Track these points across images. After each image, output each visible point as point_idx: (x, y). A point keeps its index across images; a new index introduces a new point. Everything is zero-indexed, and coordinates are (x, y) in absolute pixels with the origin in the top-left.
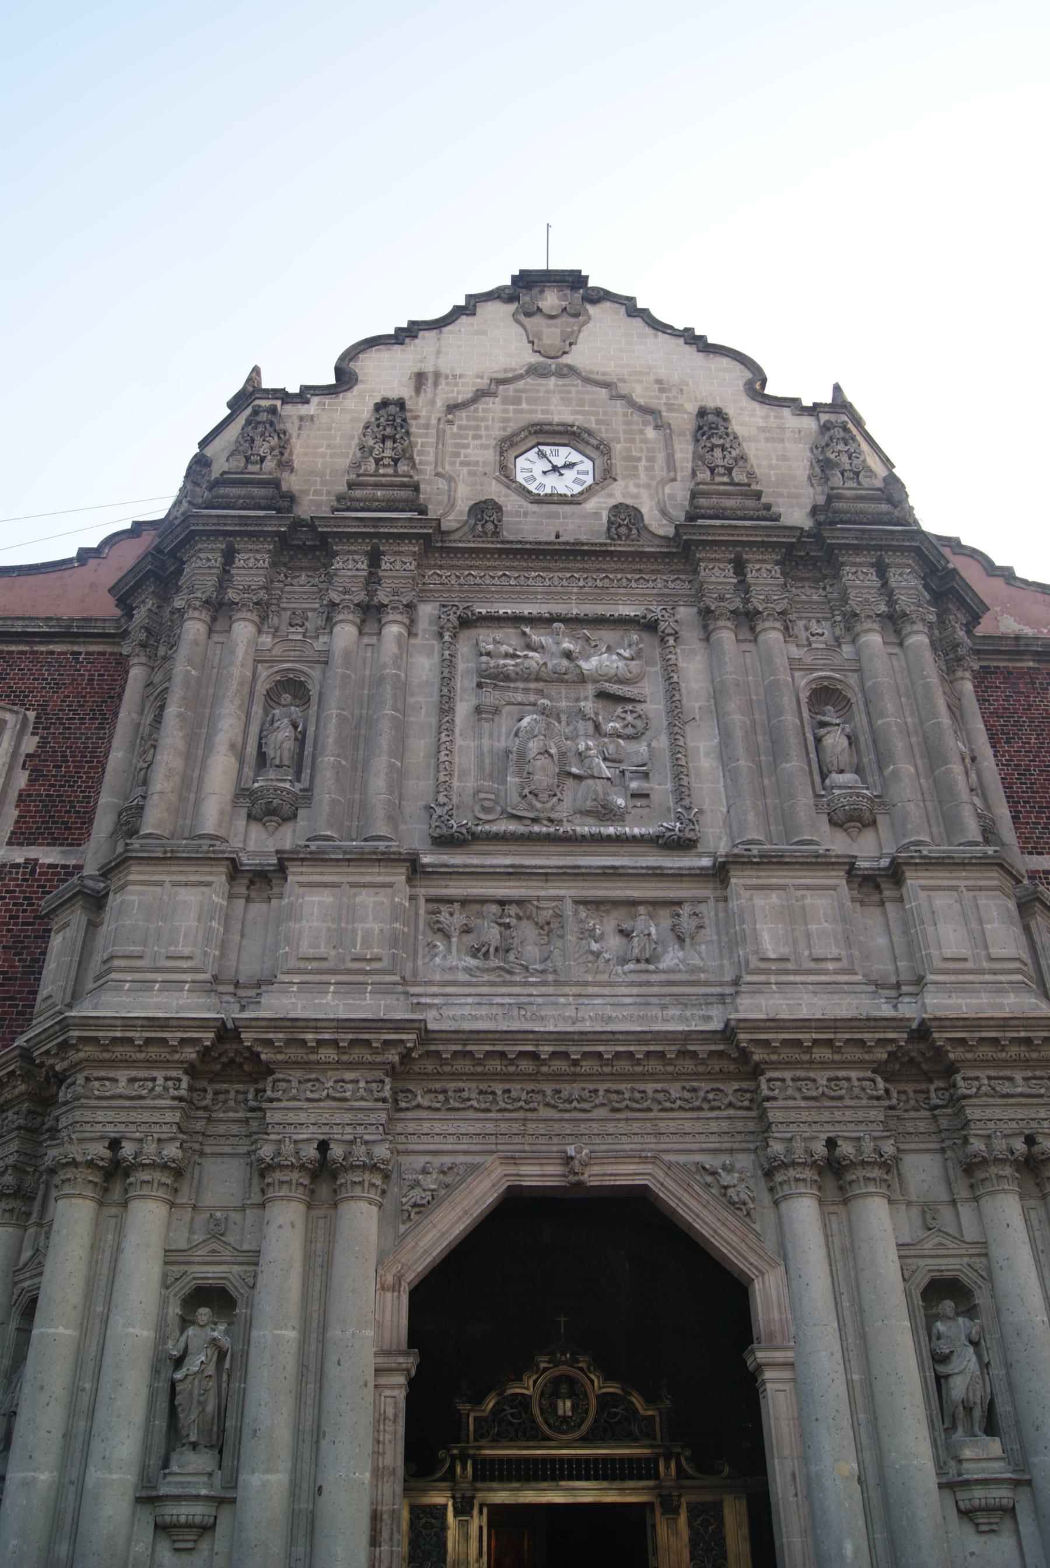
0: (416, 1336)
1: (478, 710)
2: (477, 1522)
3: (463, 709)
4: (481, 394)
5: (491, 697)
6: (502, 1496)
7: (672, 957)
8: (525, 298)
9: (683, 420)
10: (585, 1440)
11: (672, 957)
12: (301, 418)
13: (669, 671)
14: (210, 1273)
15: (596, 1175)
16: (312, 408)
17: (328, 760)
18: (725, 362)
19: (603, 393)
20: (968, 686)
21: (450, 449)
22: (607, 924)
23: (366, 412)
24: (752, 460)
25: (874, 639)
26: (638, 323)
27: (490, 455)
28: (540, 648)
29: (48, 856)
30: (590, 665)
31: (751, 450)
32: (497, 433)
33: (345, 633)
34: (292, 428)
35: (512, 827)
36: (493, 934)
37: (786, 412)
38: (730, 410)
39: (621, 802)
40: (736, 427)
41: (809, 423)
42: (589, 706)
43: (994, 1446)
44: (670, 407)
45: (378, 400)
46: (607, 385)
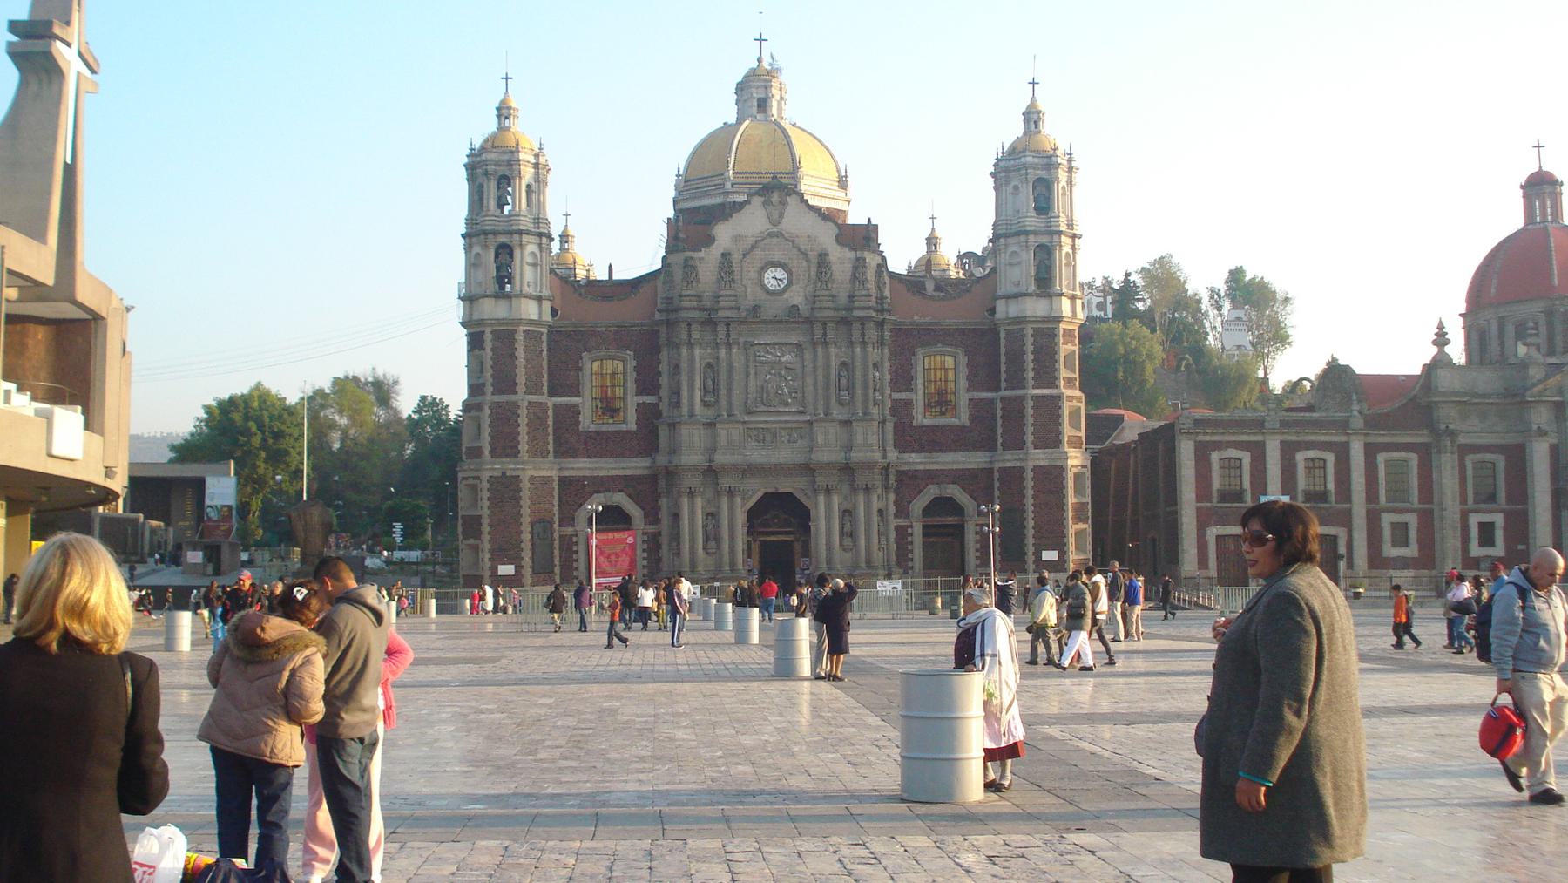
1: (756, 374)
2: (758, 543)
3: (752, 372)
4: (753, 247)
7: (800, 442)
10: (780, 527)
11: (800, 442)
12: (700, 259)
15: (781, 491)
16: (702, 254)
17: (723, 392)
18: (830, 225)
20: (886, 351)
23: (719, 257)
24: (834, 273)
25: (858, 350)
26: (803, 205)
28: (771, 353)
30: (783, 359)
31: (833, 268)
32: (759, 265)
33: (723, 352)
35: (766, 409)
37: (847, 249)
38: (830, 250)
41: (852, 255)
43: (850, 539)
44: (812, 249)
45: (722, 251)
46: (793, 242)
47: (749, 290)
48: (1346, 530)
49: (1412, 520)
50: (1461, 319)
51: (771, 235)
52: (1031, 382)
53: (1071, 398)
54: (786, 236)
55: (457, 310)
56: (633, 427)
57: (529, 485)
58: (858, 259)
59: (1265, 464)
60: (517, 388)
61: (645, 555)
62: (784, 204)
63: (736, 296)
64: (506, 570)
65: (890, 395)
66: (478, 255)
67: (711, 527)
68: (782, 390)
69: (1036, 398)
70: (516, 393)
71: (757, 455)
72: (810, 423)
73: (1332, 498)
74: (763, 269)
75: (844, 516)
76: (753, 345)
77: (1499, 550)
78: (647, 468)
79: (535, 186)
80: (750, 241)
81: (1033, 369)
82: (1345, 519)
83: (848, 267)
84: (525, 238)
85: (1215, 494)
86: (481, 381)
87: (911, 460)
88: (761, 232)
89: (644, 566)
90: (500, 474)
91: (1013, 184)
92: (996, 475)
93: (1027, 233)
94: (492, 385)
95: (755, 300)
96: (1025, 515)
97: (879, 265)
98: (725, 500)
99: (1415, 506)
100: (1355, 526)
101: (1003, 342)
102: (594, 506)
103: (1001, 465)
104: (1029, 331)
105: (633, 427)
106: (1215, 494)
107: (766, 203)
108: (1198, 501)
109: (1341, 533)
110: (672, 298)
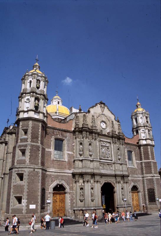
0: (101, 191)
1: (101, 148)
3: (100, 148)
7: (111, 168)
8: (101, 105)
9: (111, 121)
13: (111, 146)
14: (92, 187)
22: (108, 166)
23: (91, 116)
29: (70, 153)
30: (107, 145)
31: (115, 125)
34: (86, 116)
36: (103, 166)
47: (98, 127)
51: (102, 114)
52: (151, 159)
61: (70, 201)
62: (104, 108)
63: (96, 127)
64: (33, 207)
66: (28, 99)
70: (38, 143)
71: (103, 172)
72: (114, 163)
74: (101, 122)
78: (72, 173)
86: (26, 137)
88: (100, 113)
90: (32, 170)
92: (145, 181)
96: (155, 190)
103: (147, 178)
107: (101, 107)
110: (79, 125)
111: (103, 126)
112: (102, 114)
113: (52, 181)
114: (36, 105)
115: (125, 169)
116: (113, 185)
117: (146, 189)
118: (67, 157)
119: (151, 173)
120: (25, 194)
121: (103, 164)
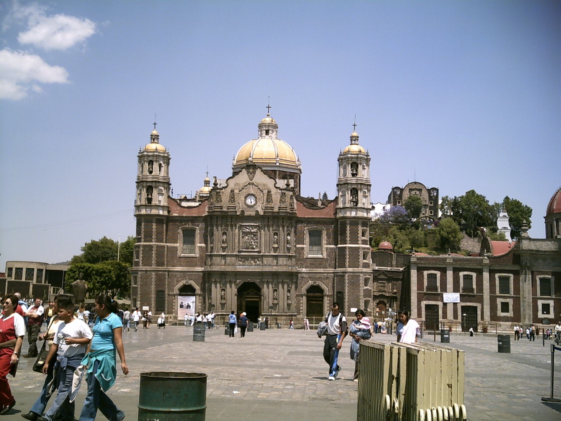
3: (241, 237)
5: (243, 235)
6: (247, 300)
9: (266, 192)
16: (223, 190)
19: (257, 188)
21: (239, 198)
23: (230, 191)
24: (273, 198)
27: (244, 198)
30: (252, 231)
31: (273, 197)
39: (255, 247)
40: (272, 193)
41: (280, 191)
42: (252, 236)
43: (276, 301)
45: (230, 189)
46: (257, 186)
47: (240, 204)
48: (481, 304)
49: (511, 301)
50: (544, 219)
51: (249, 184)
52: (348, 242)
53: (364, 248)
54: (255, 184)
55: (132, 211)
56: (198, 255)
57: (155, 276)
58: (282, 193)
59: (446, 277)
60: (153, 240)
61: (200, 304)
65: (295, 246)
67: (223, 294)
68: (252, 242)
69: (351, 247)
71: (240, 268)
73: (475, 291)
74: (246, 197)
75: (274, 292)
76: (241, 226)
77: (552, 316)
79: (163, 165)
80: (241, 186)
81: (349, 237)
82: (480, 300)
83: (279, 196)
84: (157, 184)
85: (425, 288)
87: (303, 271)
88: (246, 182)
89: (199, 309)
91: (344, 164)
93: (348, 184)
94: (144, 239)
95: (242, 208)
97: (291, 196)
98: (228, 285)
99: (512, 295)
100: (484, 303)
101: (339, 226)
102: (180, 284)
104: (348, 222)
105: (198, 255)
106: (425, 288)
107: (248, 172)
108: (417, 291)
109: (479, 306)
111: (250, 201)
112: (249, 184)
113: (178, 282)
114: (150, 197)
115: (283, 262)
116: (259, 285)
117: (335, 291)
118: (198, 251)
119: (344, 266)
120: (139, 296)
121: (246, 258)
